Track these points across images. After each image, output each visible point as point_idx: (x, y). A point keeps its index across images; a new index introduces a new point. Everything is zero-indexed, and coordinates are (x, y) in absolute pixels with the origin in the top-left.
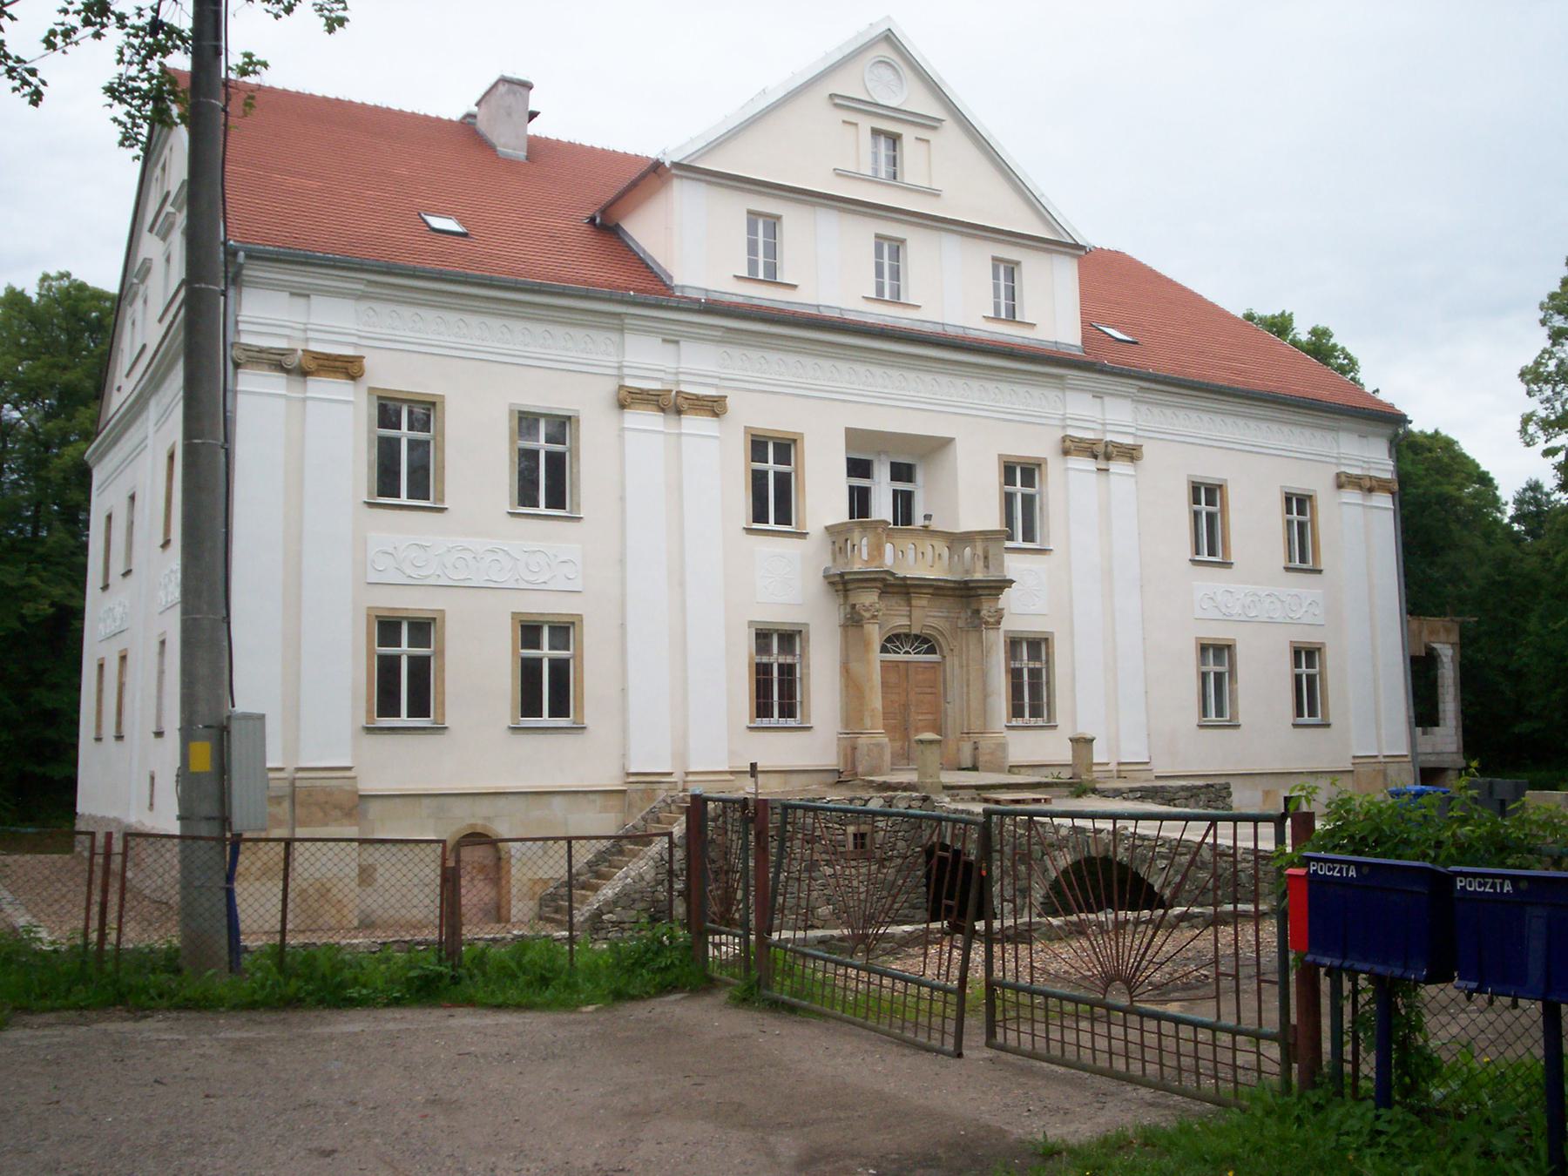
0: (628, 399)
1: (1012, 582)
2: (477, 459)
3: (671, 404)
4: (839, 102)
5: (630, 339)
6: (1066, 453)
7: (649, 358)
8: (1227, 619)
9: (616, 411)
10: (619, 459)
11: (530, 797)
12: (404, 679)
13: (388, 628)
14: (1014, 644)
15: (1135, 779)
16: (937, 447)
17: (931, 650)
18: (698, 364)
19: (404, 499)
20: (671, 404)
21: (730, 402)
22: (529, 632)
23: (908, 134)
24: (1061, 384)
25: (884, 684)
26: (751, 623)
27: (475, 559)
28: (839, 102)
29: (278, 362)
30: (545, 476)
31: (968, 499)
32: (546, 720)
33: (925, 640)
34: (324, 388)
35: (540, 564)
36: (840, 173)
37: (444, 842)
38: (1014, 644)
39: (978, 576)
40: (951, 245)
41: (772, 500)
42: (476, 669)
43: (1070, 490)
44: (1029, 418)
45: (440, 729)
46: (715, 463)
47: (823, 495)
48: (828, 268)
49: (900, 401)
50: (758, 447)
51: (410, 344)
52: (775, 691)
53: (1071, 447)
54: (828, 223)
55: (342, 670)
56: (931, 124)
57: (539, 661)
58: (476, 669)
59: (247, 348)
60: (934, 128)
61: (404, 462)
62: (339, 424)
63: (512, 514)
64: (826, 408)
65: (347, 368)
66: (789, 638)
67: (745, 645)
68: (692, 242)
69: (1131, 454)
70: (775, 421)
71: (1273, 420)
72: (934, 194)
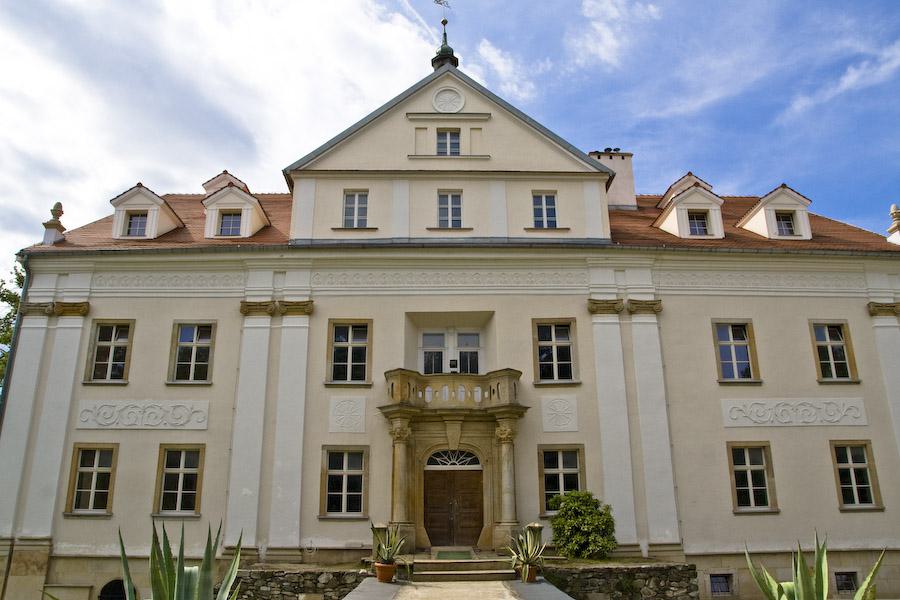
0: (248, 309)
1: (527, 408)
2: (150, 354)
3: (278, 309)
5: (252, 274)
7: (261, 284)
10: (242, 347)
13: (86, 455)
14: (549, 457)
16: (485, 319)
17: (475, 461)
18: (295, 285)
20: (278, 309)
22: (171, 456)
23: (465, 130)
26: (324, 447)
28: (412, 117)
30: (192, 363)
32: (178, 512)
33: (469, 455)
35: (185, 414)
36: (411, 157)
38: (549, 457)
39: (494, 404)
41: (348, 361)
42: (137, 477)
44: (558, 292)
45: (109, 516)
46: (303, 345)
48: (404, 213)
52: (342, 489)
53: (596, 308)
54: (401, 190)
57: (745, 472)
58: (137, 477)
60: (486, 120)
61: (109, 358)
63: (168, 385)
66: (358, 456)
67: (318, 462)
69: (653, 308)
72: (487, 158)
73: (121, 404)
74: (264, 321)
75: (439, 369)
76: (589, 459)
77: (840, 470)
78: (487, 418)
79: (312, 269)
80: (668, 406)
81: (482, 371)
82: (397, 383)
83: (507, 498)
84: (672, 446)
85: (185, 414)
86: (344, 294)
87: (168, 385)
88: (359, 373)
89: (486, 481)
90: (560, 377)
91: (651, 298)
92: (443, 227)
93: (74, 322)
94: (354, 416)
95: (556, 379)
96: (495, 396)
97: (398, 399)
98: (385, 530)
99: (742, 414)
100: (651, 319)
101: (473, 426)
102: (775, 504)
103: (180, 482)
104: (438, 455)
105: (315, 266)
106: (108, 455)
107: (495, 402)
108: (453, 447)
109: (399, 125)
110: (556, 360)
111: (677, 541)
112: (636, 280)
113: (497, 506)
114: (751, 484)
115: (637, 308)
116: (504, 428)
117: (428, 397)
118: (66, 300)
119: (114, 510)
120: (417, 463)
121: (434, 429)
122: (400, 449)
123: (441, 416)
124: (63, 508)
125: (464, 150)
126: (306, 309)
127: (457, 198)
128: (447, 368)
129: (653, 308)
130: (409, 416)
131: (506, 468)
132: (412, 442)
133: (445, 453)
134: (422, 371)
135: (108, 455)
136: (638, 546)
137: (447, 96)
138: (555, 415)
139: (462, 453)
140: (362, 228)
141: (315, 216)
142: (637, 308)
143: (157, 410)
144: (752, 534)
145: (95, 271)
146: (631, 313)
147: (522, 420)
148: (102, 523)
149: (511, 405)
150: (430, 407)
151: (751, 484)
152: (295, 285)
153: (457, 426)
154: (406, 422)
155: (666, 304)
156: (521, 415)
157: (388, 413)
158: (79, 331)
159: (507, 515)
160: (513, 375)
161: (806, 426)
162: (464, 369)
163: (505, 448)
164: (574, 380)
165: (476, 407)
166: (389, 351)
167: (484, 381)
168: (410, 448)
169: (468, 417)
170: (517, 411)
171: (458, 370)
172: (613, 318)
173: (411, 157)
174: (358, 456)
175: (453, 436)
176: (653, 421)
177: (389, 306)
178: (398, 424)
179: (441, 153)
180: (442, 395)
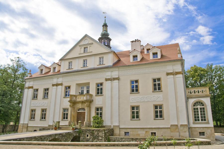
2: (41, 94)
3: (57, 85)
8: (138, 102)
10: (52, 91)
14: (97, 109)
20: (57, 85)
23: (88, 46)
27: (40, 103)
28: (80, 46)
36: (79, 54)
38: (97, 109)
40: (93, 58)
42: (38, 114)
43: (107, 86)
44: (100, 77)
46: (61, 90)
48: (77, 65)
49: (82, 79)
51: (36, 85)
53: (107, 80)
54: (77, 60)
60: (92, 44)
62: (31, 91)
66: (67, 110)
69: (118, 79)
72: (91, 52)
73: (36, 102)
74: (55, 87)
76: (104, 109)
77: (156, 111)
79: (62, 77)
80: (119, 99)
84: (119, 107)
86: (66, 81)
91: (118, 77)
92: (100, 64)
93: (31, 90)
94: (66, 103)
95: (157, 90)
99: (135, 99)
100: (117, 81)
104: (79, 109)
105: (63, 77)
108: (81, 108)
109: (78, 48)
110: (99, 91)
111: (118, 125)
112: (115, 73)
114: (135, 113)
115: (114, 79)
120: (75, 111)
121: (78, 104)
124: (29, 119)
125: (88, 51)
126: (61, 84)
129: (118, 79)
130: (73, 103)
136: (111, 126)
137: (86, 41)
138: (98, 101)
139: (82, 108)
141: (64, 68)
142: (114, 79)
143: (41, 103)
144: (135, 124)
145: (34, 81)
146: (114, 80)
148: (34, 121)
151: (135, 113)
152: (60, 80)
155: (120, 77)
158: (31, 91)
161: (148, 101)
166: (73, 92)
169: (83, 102)
172: (110, 82)
173: (79, 54)
174: (67, 110)
175: (80, 106)
176: (116, 101)
177: (73, 82)
179: (84, 52)
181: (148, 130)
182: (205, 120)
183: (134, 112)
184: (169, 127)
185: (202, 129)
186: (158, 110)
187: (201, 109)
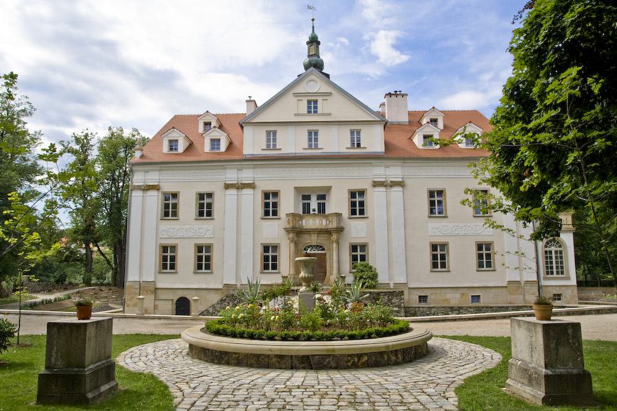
0: (227, 187)
2: (188, 206)
3: (240, 187)
4: (296, 95)
5: (227, 171)
6: (374, 186)
7: (232, 175)
8: (445, 235)
9: (224, 189)
10: (224, 203)
11: (455, 290)
12: (168, 260)
13: (165, 249)
14: (354, 248)
15: (384, 289)
16: (329, 189)
17: (323, 249)
18: (247, 175)
19: (205, 217)
20: (240, 187)
21: (256, 183)
22: (200, 249)
23: (320, 100)
24: (224, 168)
25: (577, 257)
26: (261, 244)
27: (187, 231)
28: (296, 95)
29: (139, 188)
30: (205, 209)
31: (338, 203)
32: (204, 271)
33: (321, 247)
34: (247, 192)
35: (204, 231)
36: (296, 115)
37: (172, 300)
38: (354, 248)
39: (330, 227)
40: (334, 129)
41: (270, 208)
42: (186, 258)
43: (375, 200)
44: (359, 177)
45: (176, 273)
46: (252, 201)
47: (288, 204)
48: (292, 142)
49: (313, 178)
50: (267, 195)
51: (170, 181)
52: (269, 260)
53: (376, 184)
54: (291, 131)
55: (152, 258)
56: (330, 94)
58: (186, 258)
59: (134, 186)
61: (170, 209)
62: (154, 201)
64: (286, 183)
65: (251, 186)
66: (275, 248)
67: (260, 250)
68: (253, 143)
69: (401, 184)
70: (271, 187)
71: (439, 166)
72: (329, 114)
73: (178, 227)
74: (233, 192)
75: (309, 212)
78: (328, 232)
79: (254, 168)
80: (405, 226)
81: (327, 213)
82: (291, 219)
83: (335, 265)
85: (204, 231)
86: (267, 179)
87: (196, 219)
88: (275, 213)
89: (327, 257)
90: (360, 214)
91: (400, 180)
93: (153, 193)
94: (274, 231)
96: (331, 223)
97: (291, 225)
98: (287, 277)
99: (437, 230)
100: (400, 189)
101: (322, 235)
102: (449, 268)
103: (204, 260)
105: (255, 167)
106: (174, 248)
107: (330, 226)
109: (290, 99)
110: (357, 206)
112: (394, 172)
113: (332, 267)
114: (439, 256)
115: (394, 184)
116: (334, 237)
117: (304, 224)
118: (149, 184)
119: (178, 270)
121: (306, 236)
122: (292, 245)
123: (309, 232)
124: (158, 270)
125: (319, 111)
126: (251, 186)
127: (316, 133)
128: (312, 212)
129: (401, 184)
130: (297, 232)
131: (335, 253)
132: (297, 242)
133: (311, 246)
134: (301, 213)
135: (174, 248)
137: (312, 83)
138: (357, 230)
140: (275, 149)
141: (253, 143)
142: (394, 184)
143: (192, 230)
144: (439, 279)
145: (160, 170)
146: (391, 186)
147: (342, 233)
149: (337, 228)
150: (305, 228)
151: (439, 256)
152: (247, 175)
153: (316, 236)
154: (295, 234)
155: (407, 182)
156: (342, 231)
157: (287, 231)
158: (156, 197)
159: (335, 271)
160: (339, 215)
161: (465, 235)
162: (319, 212)
163: (334, 245)
164: (365, 216)
165: (323, 228)
166: (288, 204)
167: (327, 217)
168: (296, 244)
169: (320, 232)
170: (340, 230)
171: (316, 212)
172: (383, 189)
173: (296, 115)
174: (275, 248)
175: (314, 239)
176: (398, 234)
177: (286, 183)
178: (291, 235)
179: (309, 112)
180: (310, 223)
181: (465, 291)
182: (562, 273)
183: (437, 255)
184: (505, 285)
185: (558, 288)
186: (484, 252)
187: (556, 252)
